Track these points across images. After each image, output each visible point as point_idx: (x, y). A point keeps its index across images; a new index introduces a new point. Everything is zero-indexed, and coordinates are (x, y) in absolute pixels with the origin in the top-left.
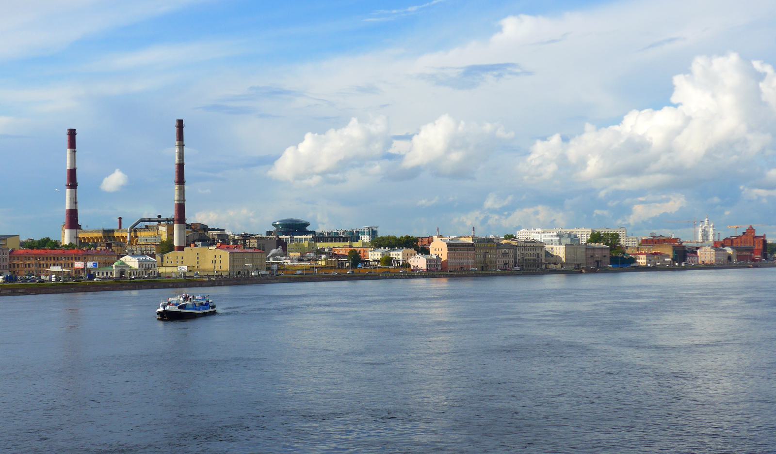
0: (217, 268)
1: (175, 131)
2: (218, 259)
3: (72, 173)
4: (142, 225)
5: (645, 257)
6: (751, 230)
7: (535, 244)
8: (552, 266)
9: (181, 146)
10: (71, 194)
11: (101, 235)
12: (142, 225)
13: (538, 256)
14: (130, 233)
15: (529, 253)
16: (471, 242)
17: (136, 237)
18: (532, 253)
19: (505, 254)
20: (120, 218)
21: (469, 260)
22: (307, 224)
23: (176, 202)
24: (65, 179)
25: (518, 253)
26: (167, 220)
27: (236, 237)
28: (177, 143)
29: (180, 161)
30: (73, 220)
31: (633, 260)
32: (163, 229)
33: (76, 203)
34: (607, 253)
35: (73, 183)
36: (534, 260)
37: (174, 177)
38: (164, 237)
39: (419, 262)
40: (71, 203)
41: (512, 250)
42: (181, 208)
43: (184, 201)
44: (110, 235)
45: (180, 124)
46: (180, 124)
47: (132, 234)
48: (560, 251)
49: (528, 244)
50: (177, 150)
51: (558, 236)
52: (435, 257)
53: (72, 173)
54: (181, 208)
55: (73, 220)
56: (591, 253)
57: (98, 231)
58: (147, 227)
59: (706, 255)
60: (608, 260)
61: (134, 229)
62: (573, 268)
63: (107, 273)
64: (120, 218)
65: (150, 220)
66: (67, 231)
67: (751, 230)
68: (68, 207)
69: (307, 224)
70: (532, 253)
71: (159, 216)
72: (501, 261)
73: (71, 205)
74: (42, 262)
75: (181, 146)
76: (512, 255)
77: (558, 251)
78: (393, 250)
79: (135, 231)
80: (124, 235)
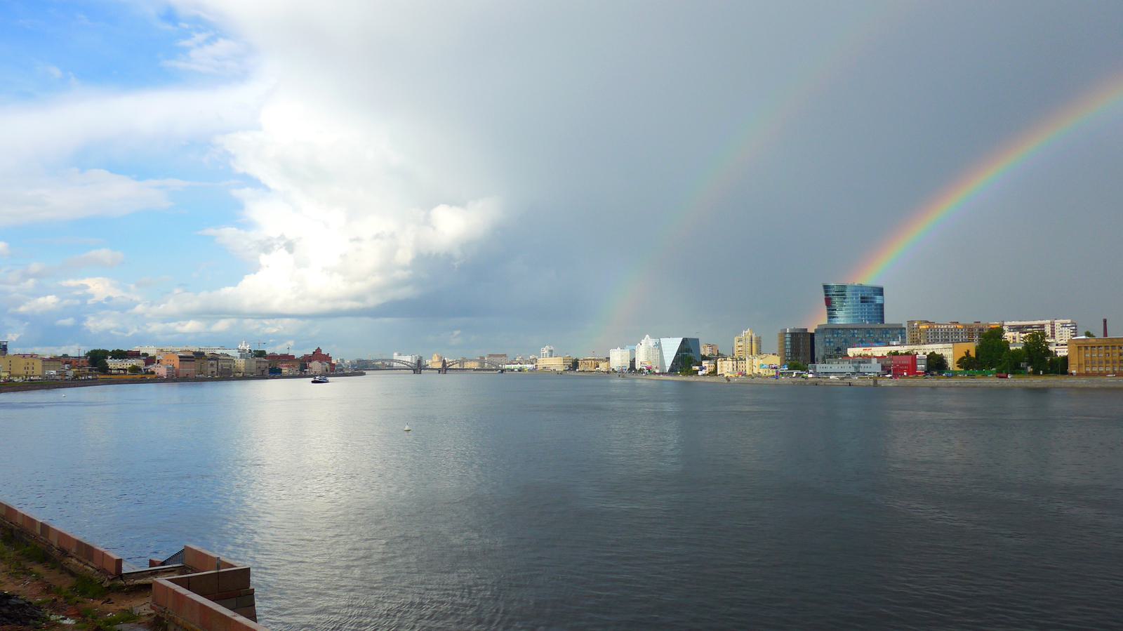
6: (319, 350)
7: (227, 358)
8: (237, 374)
16: (192, 355)
19: (212, 365)
21: (190, 369)
25: (219, 364)
31: (280, 371)
34: (267, 365)
39: (161, 370)
41: (216, 362)
48: (241, 363)
52: (171, 366)
60: (267, 370)
62: (174, 378)
67: (319, 350)
72: (210, 369)
76: (215, 366)
77: (239, 362)
78: (126, 361)
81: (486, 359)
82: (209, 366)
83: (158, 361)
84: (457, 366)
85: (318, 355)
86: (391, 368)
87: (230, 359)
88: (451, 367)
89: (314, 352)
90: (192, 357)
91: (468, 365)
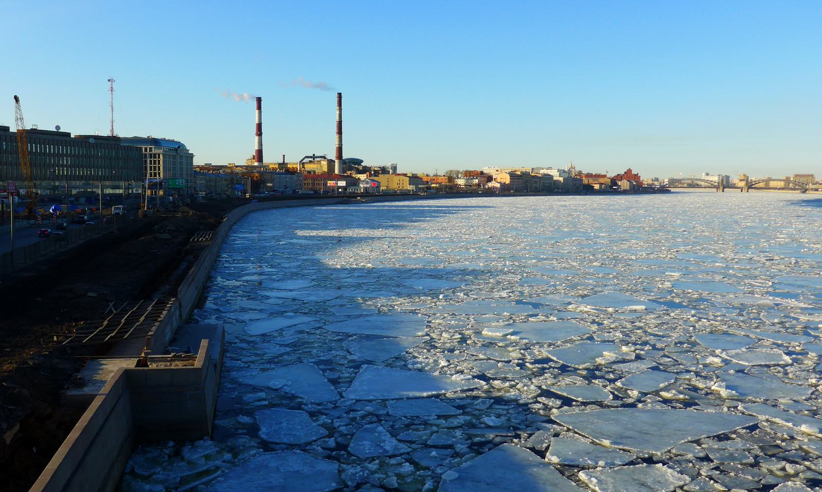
0: (401, 188)
1: (336, 100)
2: (401, 180)
3: (259, 126)
4: (306, 160)
5: (598, 185)
6: (630, 171)
9: (340, 110)
10: (259, 140)
11: (277, 166)
12: (306, 160)
13: (551, 183)
14: (300, 165)
15: (546, 181)
17: (303, 167)
18: (548, 181)
19: (536, 182)
20: (284, 156)
22: (362, 161)
23: (337, 146)
24: (254, 129)
25: (542, 182)
26: (321, 157)
27: (376, 169)
28: (338, 108)
29: (340, 119)
30: (259, 155)
32: (324, 163)
33: (262, 145)
35: (259, 132)
36: (549, 186)
37: (335, 130)
38: (325, 169)
40: (259, 145)
42: (340, 150)
43: (342, 145)
44: (283, 166)
45: (340, 95)
46: (340, 95)
47: (301, 166)
49: (547, 176)
50: (338, 112)
51: (558, 171)
53: (259, 126)
54: (340, 150)
55: (259, 155)
56: (574, 182)
57: (275, 164)
58: (311, 161)
59: (624, 184)
61: (302, 163)
63: (355, 189)
64: (284, 156)
65: (311, 157)
66: (256, 164)
67: (630, 171)
68: (257, 148)
69: (362, 161)
70: (548, 181)
71: (314, 155)
72: (534, 185)
73: (259, 147)
74: (316, 182)
75: (340, 110)
79: (303, 164)
80: (294, 166)
81: (792, 179)
82: (533, 182)
83: (495, 179)
84: (762, 185)
85: (628, 175)
86: (699, 186)
87: (550, 177)
88: (757, 186)
89: (625, 173)
90: (521, 176)
91: (772, 184)
